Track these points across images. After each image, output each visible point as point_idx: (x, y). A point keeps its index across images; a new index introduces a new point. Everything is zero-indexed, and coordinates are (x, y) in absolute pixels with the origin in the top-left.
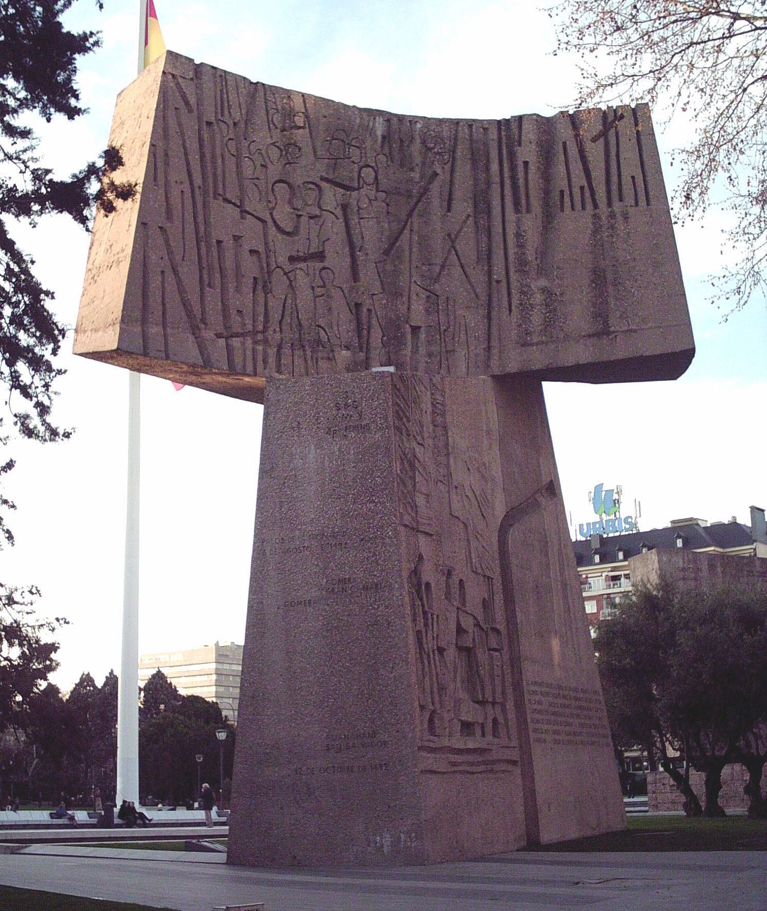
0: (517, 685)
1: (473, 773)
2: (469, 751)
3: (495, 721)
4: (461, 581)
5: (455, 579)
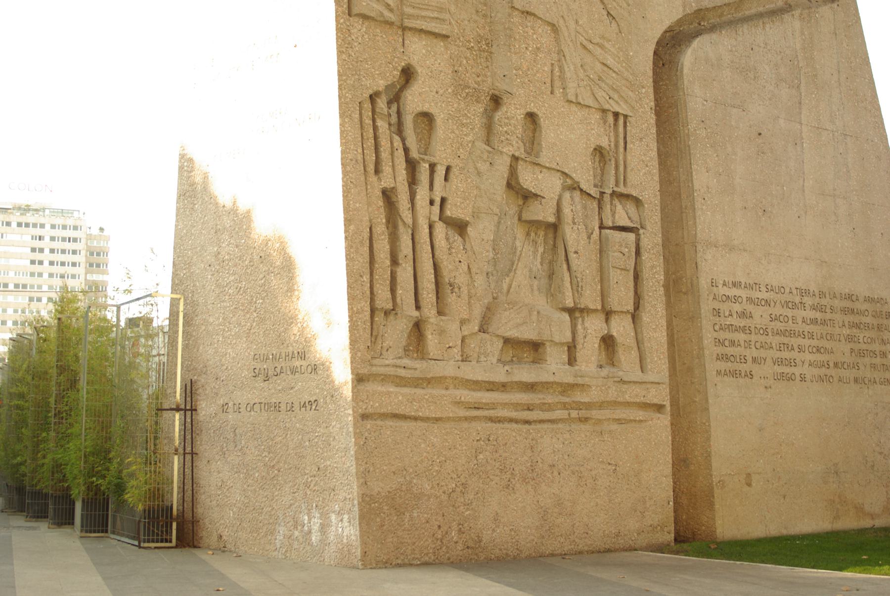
0: (679, 285)
1: (527, 422)
2: (531, 387)
3: (608, 342)
4: (531, 117)
5: (512, 114)
